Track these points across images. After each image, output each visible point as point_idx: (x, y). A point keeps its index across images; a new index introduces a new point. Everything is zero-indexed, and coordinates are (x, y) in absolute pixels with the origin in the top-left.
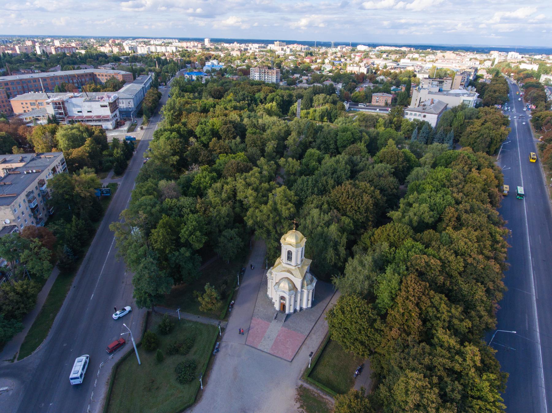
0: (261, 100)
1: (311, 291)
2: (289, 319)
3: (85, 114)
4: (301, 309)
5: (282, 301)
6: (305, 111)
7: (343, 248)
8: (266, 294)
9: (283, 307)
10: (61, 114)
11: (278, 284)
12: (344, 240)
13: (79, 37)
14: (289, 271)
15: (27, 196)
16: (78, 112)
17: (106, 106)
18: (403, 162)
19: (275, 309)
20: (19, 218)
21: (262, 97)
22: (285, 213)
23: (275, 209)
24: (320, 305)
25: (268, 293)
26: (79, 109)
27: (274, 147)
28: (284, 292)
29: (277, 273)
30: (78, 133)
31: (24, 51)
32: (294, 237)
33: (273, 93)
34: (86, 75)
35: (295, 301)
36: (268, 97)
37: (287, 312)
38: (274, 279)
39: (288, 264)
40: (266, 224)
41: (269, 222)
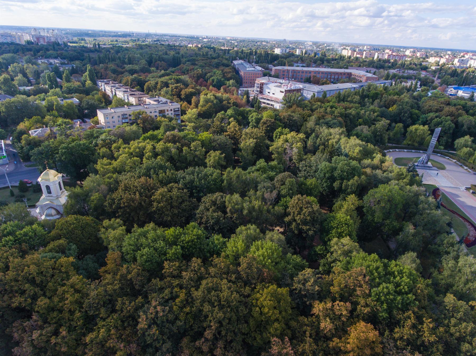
0: (427, 121)
3: (271, 95)
6: (465, 150)
10: (258, 91)
13: (438, 49)
15: (123, 115)
16: (269, 93)
17: (283, 92)
18: (305, 222)
20: (109, 122)
21: (429, 118)
26: (269, 91)
27: (250, 144)
30: (212, 99)
31: (368, 56)
33: (449, 117)
34: (344, 74)
36: (436, 120)
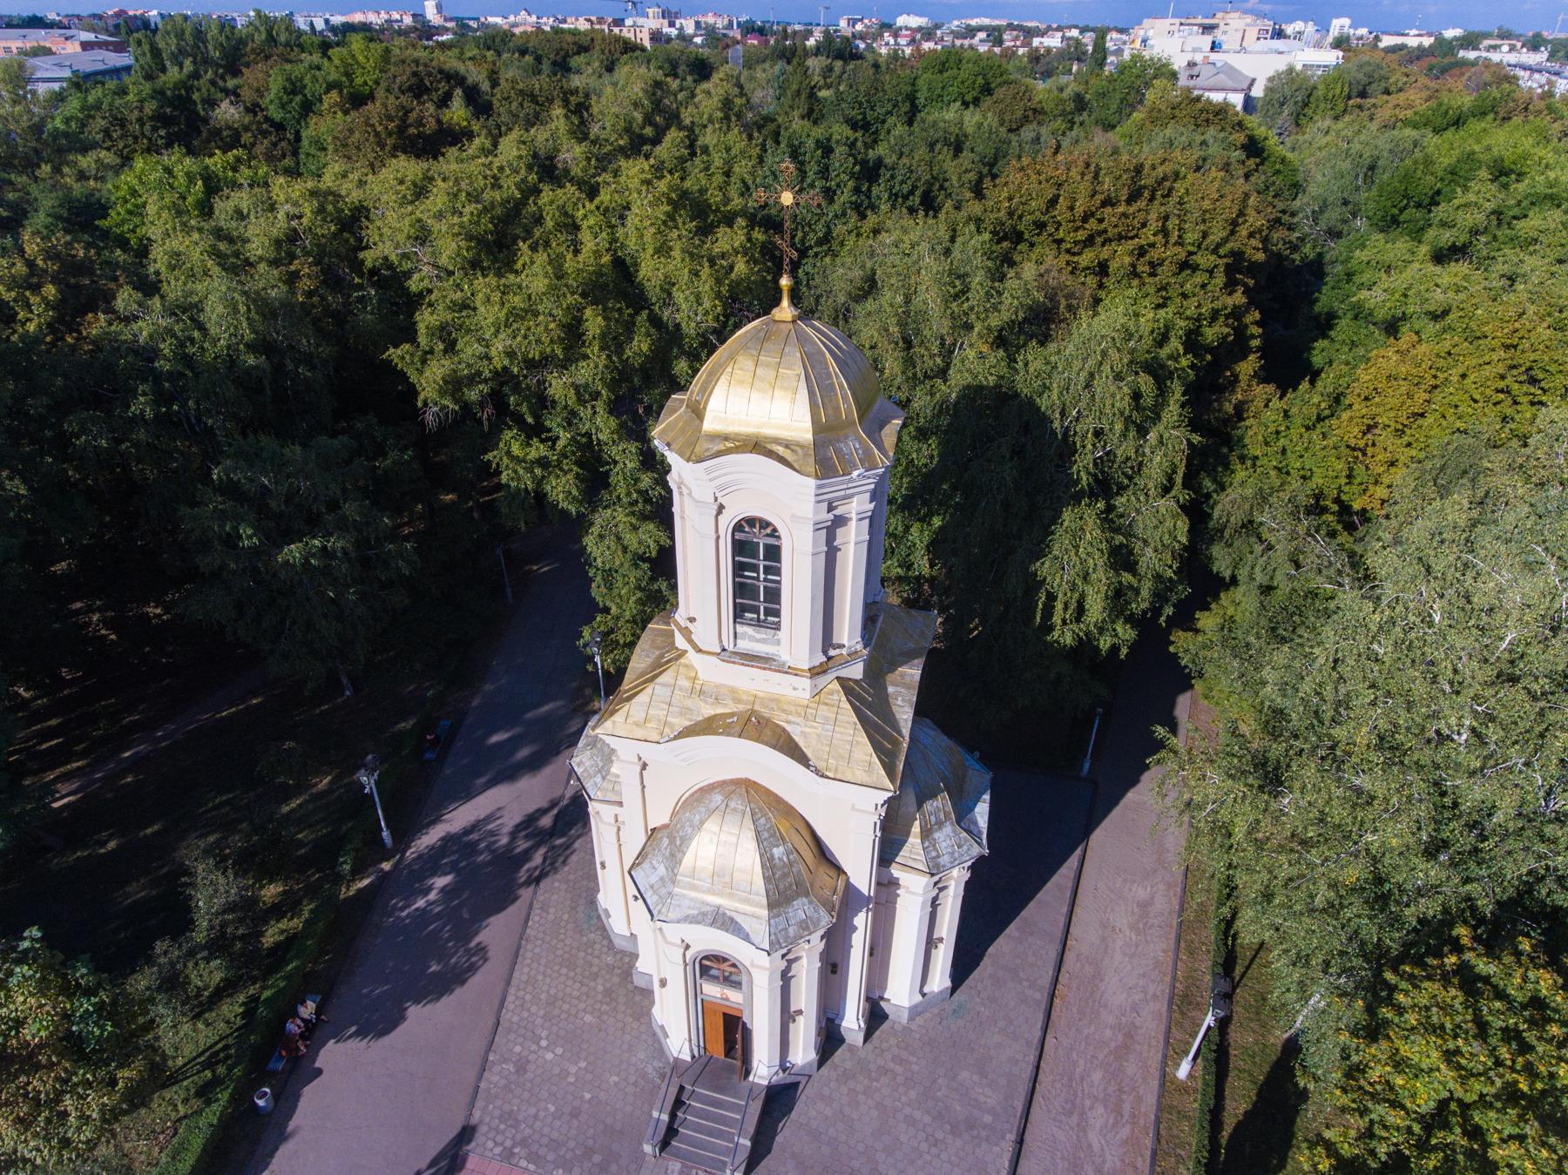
1: (957, 879)
2: (787, 1134)
4: (875, 1015)
5: (712, 990)
7: (1166, 505)
8: (593, 903)
9: (733, 1032)
11: (664, 841)
12: (1169, 440)
14: (757, 726)
19: (655, 1040)
22: (691, 308)
23: (618, 284)
24: (1002, 948)
25: (602, 898)
28: (723, 921)
29: (647, 751)
32: (794, 371)
35: (833, 968)
37: (763, 1069)
38: (630, 794)
39: (750, 659)
40: (558, 386)
41: (584, 372)
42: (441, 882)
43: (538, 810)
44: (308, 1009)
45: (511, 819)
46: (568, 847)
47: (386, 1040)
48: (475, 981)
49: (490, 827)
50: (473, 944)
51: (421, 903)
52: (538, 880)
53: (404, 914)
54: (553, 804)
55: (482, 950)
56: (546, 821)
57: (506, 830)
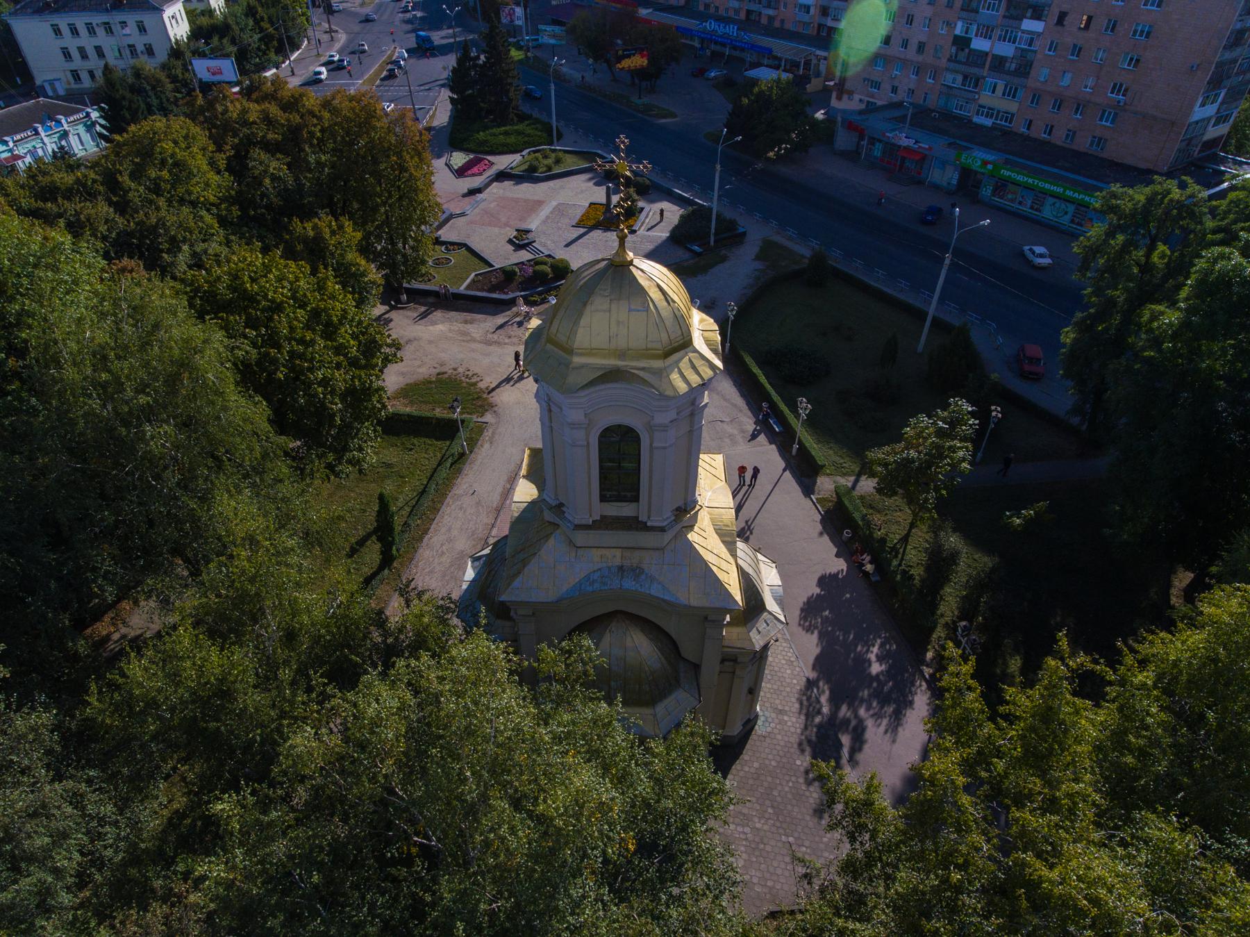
42: (876, 668)
43: (860, 750)
44: (869, 568)
45: (875, 732)
46: (807, 715)
47: (819, 575)
48: (798, 612)
49: (885, 722)
50: (816, 632)
51: (875, 649)
52: (810, 684)
53: (879, 641)
54: (853, 761)
55: (809, 630)
56: (845, 740)
57: (869, 723)
